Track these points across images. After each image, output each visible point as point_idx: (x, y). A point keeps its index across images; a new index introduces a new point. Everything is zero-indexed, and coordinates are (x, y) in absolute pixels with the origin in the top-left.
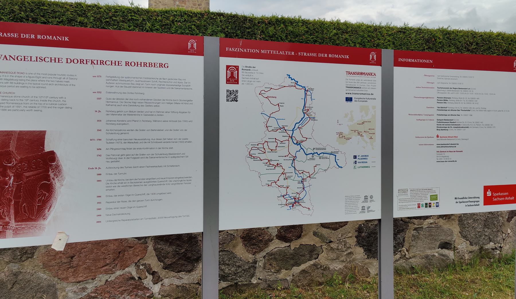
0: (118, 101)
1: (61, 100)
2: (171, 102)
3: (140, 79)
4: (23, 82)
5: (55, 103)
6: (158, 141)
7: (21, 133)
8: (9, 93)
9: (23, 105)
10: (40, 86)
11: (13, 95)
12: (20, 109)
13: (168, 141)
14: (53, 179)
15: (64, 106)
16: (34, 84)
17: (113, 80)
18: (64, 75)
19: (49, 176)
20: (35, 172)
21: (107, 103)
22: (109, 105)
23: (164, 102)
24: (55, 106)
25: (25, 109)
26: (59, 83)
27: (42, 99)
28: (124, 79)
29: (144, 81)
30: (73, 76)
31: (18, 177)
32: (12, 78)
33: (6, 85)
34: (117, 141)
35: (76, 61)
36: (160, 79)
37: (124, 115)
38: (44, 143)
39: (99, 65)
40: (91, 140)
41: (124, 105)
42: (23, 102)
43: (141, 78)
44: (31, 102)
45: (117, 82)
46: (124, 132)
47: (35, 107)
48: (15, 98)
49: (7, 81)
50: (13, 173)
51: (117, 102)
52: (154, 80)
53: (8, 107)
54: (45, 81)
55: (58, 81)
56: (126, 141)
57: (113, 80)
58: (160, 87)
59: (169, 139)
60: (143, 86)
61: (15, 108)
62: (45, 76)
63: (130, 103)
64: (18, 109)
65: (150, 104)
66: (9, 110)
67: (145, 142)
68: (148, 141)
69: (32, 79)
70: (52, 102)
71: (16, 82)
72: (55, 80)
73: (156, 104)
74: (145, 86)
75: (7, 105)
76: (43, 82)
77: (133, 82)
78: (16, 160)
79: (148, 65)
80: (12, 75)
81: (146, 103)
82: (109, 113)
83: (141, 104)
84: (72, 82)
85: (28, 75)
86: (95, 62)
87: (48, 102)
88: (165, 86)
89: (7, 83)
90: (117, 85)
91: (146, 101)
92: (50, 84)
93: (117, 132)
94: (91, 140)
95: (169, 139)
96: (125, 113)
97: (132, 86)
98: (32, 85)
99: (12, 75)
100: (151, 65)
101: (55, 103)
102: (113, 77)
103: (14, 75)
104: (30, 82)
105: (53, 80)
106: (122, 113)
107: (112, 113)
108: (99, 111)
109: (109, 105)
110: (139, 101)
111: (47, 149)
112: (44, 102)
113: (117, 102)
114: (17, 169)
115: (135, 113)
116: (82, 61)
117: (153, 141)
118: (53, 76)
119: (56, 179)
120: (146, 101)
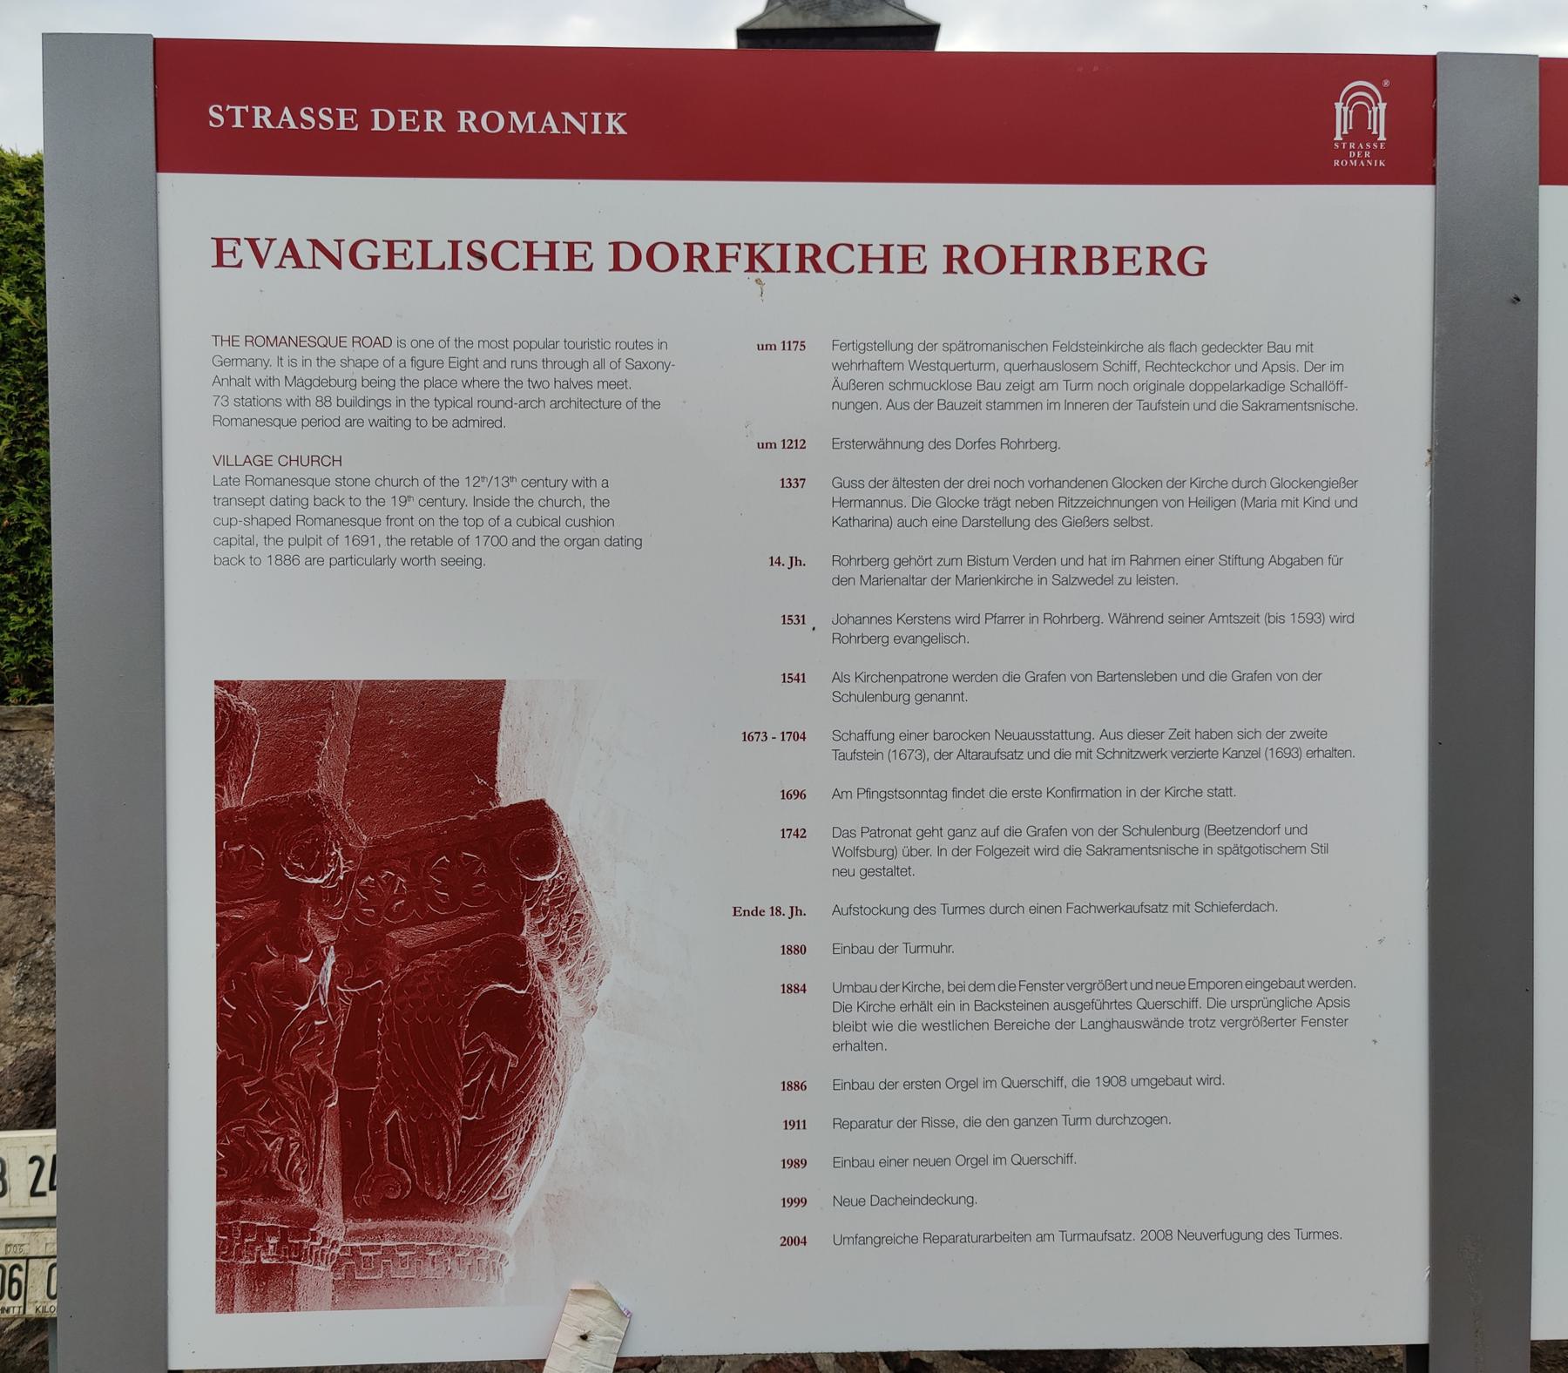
0: (904, 494)
1: (585, 494)
2: (1218, 494)
3: (1027, 357)
4: (381, 393)
5: (551, 512)
6: (1141, 744)
7: (375, 695)
8: (311, 460)
9: (381, 533)
10: (476, 413)
11: (333, 472)
12: (366, 552)
13: (1204, 745)
14: (544, 969)
15: (602, 533)
16: (443, 404)
17: (875, 366)
18: (600, 344)
19: (520, 950)
20: (448, 928)
21: (840, 512)
22: (849, 522)
23: (1176, 494)
24: (551, 533)
25: (395, 552)
26: (575, 394)
27: (484, 492)
28: (939, 355)
29: (1060, 367)
30: (647, 345)
31: (360, 953)
32: (325, 373)
33: (298, 413)
34: (899, 745)
35: (662, 257)
36: (1154, 348)
37: (940, 581)
38: (494, 754)
39: (793, 277)
40: (747, 737)
41: (938, 523)
42: (380, 512)
43: (1037, 347)
44: (428, 512)
45: (896, 376)
46: (937, 688)
47: (445, 542)
48: (345, 492)
49: (302, 392)
50: (333, 926)
51: (898, 504)
52: (1115, 357)
53: (306, 542)
54: (495, 384)
55: (567, 385)
56: (946, 746)
57: (875, 366)
58: (1152, 399)
59: (1208, 735)
60: (1051, 395)
61: (344, 550)
62: (497, 354)
63: (973, 504)
64: (359, 551)
65: (1094, 513)
66: (311, 561)
67: (1063, 755)
68: (1080, 745)
69: (428, 373)
70: (536, 512)
71: (346, 393)
72: (550, 374)
73: (1131, 511)
74: (1060, 395)
75: (299, 531)
76: (491, 394)
77: (988, 376)
78: (348, 853)
79: (1080, 262)
80: (327, 353)
81: (1068, 502)
82: (854, 571)
83: (1033, 514)
84: (643, 384)
85: (406, 353)
86: (772, 257)
87: (511, 512)
88: (1187, 396)
89: (301, 401)
90: (898, 397)
91: (1067, 492)
92: (525, 404)
93: (894, 688)
94: (747, 737)
95: (1208, 735)
96: (945, 572)
97: (987, 396)
98: (432, 412)
99: (327, 353)
100: (1096, 260)
101: (551, 512)
102: (877, 346)
103: (336, 353)
104: (420, 393)
105: (539, 374)
106: (929, 572)
107: (867, 571)
108: (795, 562)
109: (849, 522)
110: (1025, 493)
111: (511, 790)
112: (493, 512)
113: (898, 504)
114: (356, 907)
115: (1000, 571)
116: (696, 257)
117: (1109, 745)
118: (537, 355)
119: (559, 973)
120: (1067, 492)
